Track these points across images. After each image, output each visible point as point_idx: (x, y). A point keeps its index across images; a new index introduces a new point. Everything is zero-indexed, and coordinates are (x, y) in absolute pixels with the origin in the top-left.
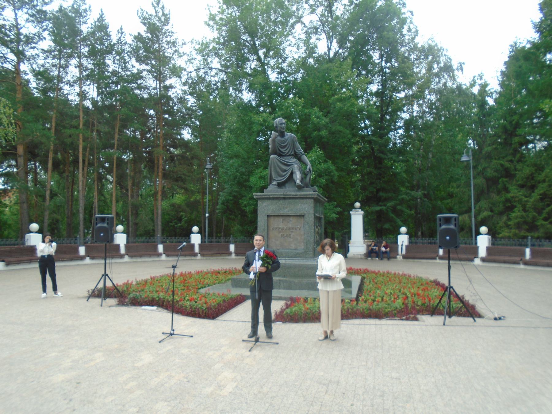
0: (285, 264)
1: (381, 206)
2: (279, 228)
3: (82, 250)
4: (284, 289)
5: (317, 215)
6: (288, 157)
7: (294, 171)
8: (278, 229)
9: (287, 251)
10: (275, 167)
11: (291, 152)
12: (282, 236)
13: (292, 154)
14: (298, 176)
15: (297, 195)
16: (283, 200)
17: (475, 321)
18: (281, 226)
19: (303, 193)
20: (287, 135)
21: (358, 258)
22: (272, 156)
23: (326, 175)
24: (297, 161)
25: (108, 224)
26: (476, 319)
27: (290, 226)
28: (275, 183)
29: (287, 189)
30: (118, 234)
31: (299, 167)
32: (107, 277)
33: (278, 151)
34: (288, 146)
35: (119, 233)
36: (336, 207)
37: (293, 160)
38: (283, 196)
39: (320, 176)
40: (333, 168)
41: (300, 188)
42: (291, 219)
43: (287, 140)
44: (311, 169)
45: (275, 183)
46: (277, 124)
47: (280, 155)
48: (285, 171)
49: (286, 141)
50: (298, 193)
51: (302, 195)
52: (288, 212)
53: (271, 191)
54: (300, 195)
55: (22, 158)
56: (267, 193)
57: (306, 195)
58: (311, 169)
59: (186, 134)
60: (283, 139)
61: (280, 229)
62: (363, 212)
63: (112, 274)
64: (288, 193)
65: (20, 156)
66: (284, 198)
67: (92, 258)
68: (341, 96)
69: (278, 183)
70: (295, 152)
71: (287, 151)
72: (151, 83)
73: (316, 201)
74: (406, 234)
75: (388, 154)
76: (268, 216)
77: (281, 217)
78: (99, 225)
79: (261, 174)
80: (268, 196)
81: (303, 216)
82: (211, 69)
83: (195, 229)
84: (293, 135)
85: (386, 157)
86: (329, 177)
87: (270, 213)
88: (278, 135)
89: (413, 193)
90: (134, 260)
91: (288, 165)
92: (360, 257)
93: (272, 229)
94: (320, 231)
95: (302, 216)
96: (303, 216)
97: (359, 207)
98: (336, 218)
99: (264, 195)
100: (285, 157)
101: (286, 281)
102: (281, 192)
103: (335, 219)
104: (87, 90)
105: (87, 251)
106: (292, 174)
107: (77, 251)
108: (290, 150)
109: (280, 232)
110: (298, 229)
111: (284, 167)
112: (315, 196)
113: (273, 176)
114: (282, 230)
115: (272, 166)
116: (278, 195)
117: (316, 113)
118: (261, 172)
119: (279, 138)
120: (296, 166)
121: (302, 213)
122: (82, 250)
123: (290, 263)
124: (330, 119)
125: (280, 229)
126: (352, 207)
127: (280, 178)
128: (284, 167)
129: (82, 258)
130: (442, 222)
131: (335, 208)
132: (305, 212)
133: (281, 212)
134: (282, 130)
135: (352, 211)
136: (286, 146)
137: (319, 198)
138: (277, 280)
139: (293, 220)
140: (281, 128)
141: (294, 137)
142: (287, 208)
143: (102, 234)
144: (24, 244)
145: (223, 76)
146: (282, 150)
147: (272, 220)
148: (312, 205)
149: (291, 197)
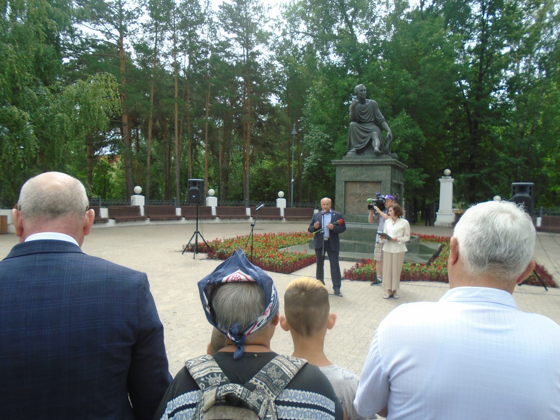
0: (361, 228)
1: (475, 173)
2: (357, 194)
3: (178, 212)
4: (358, 252)
5: (394, 181)
6: (368, 124)
7: (373, 138)
9: (364, 216)
10: (354, 134)
12: (359, 202)
13: (372, 120)
14: (377, 143)
16: (361, 167)
17: (547, 290)
18: (358, 192)
20: (368, 101)
21: (446, 227)
22: (351, 123)
23: (414, 140)
26: (548, 288)
27: (367, 192)
28: (353, 150)
29: (366, 156)
30: (210, 197)
31: (378, 133)
32: (198, 235)
33: (358, 118)
36: (422, 173)
37: (372, 127)
38: (360, 163)
39: (407, 141)
40: (421, 133)
41: (378, 155)
43: (368, 106)
44: (391, 135)
45: (353, 150)
46: (357, 91)
47: (360, 121)
48: (364, 138)
50: (376, 160)
51: (380, 162)
52: (365, 179)
53: (349, 158)
54: (377, 162)
55: (127, 126)
56: (345, 160)
57: (384, 162)
58: (391, 135)
59: (274, 100)
60: (364, 106)
62: (453, 179)
63: (202, 232)
64: (366, 160)
65: (125, 125)
66: (362, 165)
67: (187, 219)
68: (431, 56)
69: (357, 150)
70: (376, 119)
71: (367, 118)
73: (394, 167)
75: (485, 117)
76: (346, 182)
83: (281, 193)
84: (374, 101)
85: (482, 120)
86: (417, 143)
87: (347, 179)
88: (358, 102)
89: (512, 160)
90: (225, 221)
92: (448, 226)
94: (399, 198)
95: (379, 182)
97: (449, 174)
98: (423, 184)
99: (342, 162)
100: (365, 124)
101: (361, 244)
102: (359, 159)
103: (422, 186)
105: (183, 212)
106: (371, 140)
107: (174, 212)
109: (357, 198)
111: (363, 134)
112: (393, 163)
113: (352, 144)
115: (351, 133)
116: (357, 162)
117: (404, 75)
118: (345, 138)
119: (359, 105)
120: (375, 133)
121: (379, 179)
122: (178, 212)
123: (366, 227)
124: (420, 81)
126: (442, 174)
127: (359, 145)
128: (363, 134)
129: (179, 218)
130: (516, 191)
131: (421, 175)
132: (383, 179)
133: (358, 179)
135: (441, 178)
137: (398, 165)
138: (352, 243)
139: (370, 186)
140: (361, 94)
141: (375, 103)
142: (364, 175)
143: (194, 196)
144: (130, 204)
145: (310, 40)
146: (363, 117)
147: (349, 185)
148: (389, 172)
149: (368, 163)
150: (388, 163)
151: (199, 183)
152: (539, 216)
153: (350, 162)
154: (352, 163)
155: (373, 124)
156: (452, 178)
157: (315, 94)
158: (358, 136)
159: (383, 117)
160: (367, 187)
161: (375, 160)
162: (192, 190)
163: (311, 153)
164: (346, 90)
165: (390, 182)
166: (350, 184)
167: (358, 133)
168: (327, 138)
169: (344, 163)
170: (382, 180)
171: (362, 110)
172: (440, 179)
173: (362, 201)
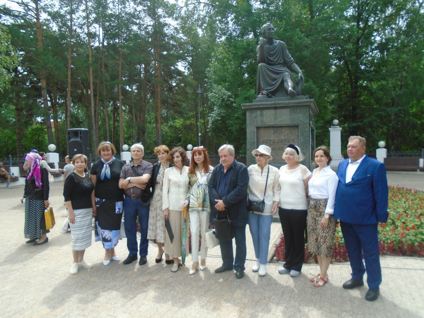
1: (357, 122)
6: (277, 66)
7: (285, 79)
8: (268, 142)
11: (280, 61)
13: (281, 62)
14: (290, 85)
15: (290, 103)
18: (272, 138)
19: (297, 101)
20: (276, 42)
22: (260, 64)
24: (288, 70)
25: (81, 139)
27: (283, 138)
30: (124, 152)
34: (277, 54)
35: (125, 151)
38: (274, 106)
41: (292, 95)
43: (276, 47)
47: (270, 63)
48: (275, 79)
49: (275, 48)
52: (279, 123)
53: (260, 101)
54: (293, 103)
55: (45, 90)
56: (255, 103)
57: (301, 103)
59: (181, 66)
60: (271, 47)
61: (272, 142)
62: (341, 128)
65: (43, 89)
68: (323, 16)
70: (284, 59)
71: (276, 59)
72: (148, 21)
74: (385, 147)
75: (365, 73)
76: (257, 128)
77: (272, 128)
78: (72, 140)
79: (246, 95)
81: (297, 126)
84: (282, 42)
85: (363, 76)
87: (259, 124)
88: (266, 41)
89: (389, 109)
93: (262, 141)
96: (297, 126)
102: (271, 102)
106: (283, 82)
108: (279, 57)
111: (274, 76)
114: (274, 142)
116: (268, 104)
119: (267, 46)
120: (287, 73)
121: (296, 123)
125: (272, 142)
126: (330, 123)
128: (274, 76)
132: (300, 122)
134: (270, 36)
135: (330, 127)
136: (275, 53)
139: (286, 131)
140: (269, 33)
141: (283, 44)
146: (271, 58)
147: (262, 131)
149: (283, 105)
150: (306, 104)
151: (81, 132)
152: (421, 158)
153: (261, 105)
154: (264, 106)
155: (283, 66)
156: (340, 127)
157: (217, 60)
158: (267, 77)
159: (292, 59)
160: (282, 132)
161: (291, 101)
162: (73, 141)
163: (215, 109)
164: (245, 49)
166: (262, 130)
168: (228, 95)
169: (255, 107)
170: (299, 124)
171: (270, 51)
172: (330, 129)
173: (277, 148)
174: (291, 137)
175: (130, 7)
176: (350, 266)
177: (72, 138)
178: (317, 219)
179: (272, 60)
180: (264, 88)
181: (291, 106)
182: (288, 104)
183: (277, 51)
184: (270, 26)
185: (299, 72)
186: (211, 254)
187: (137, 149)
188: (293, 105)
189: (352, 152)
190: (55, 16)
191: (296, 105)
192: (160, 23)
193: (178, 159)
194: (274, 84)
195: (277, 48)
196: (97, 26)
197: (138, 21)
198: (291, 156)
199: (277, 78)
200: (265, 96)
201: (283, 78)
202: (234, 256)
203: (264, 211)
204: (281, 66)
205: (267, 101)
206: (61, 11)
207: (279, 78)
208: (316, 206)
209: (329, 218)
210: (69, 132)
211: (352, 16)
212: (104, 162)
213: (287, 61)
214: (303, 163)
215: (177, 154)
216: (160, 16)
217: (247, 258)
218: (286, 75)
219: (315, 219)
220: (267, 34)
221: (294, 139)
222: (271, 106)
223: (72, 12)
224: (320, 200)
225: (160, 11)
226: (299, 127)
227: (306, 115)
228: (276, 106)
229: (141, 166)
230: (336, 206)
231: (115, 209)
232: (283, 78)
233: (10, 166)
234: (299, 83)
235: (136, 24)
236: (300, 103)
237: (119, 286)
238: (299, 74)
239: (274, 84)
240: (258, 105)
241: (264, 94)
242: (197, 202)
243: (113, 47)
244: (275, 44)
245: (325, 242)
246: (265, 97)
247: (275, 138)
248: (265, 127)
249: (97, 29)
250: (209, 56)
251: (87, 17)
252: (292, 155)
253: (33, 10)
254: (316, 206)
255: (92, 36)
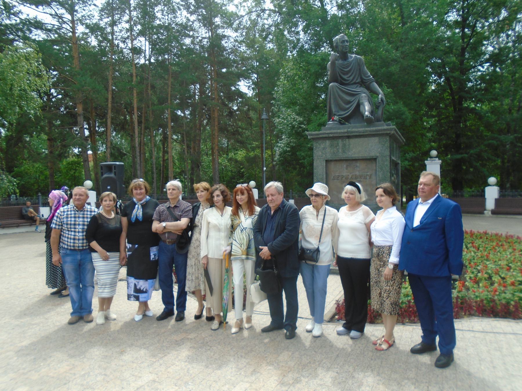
1: (462, 154)
2: (343, 177)
5: (393, 158)
7: (361, 101)
8: (340, 178)
11: (357, 80)
13: (357, 81)
14: (367, 109)
15: (366, 131)
18: (344, 174)
19: (374, 129)
20: (352, 57)
22: (331, 84)
23: (397, 118)
24: (366, 91)
25: (115, 174)
27: (357, 173)
31: (368, 96)
33: (339, 78)
34: (352, 71)
38: (346, 135)
41: (369, 122)
42: (358, 165)
43: (351, 63)
45: (336, 118)
48: (349, 102)
49: (351, 64)
51: (373, 131)
52: (353, 156)
53: (330, 129)
54: (370, 131)
55: (82, 117)
56: (324, 131)
57: (379, 130)
60: (346, 63)
62: (441, 161)
64: (354, 130)
65: (79, 115)
70: (361, 78)
71: (351, 78)
72: (203, 33)
73: (392, 137)
75: (472, 92)
76: (327, 161)
77: (344, 162)
78: (105, 176)
79: (321, 121)
80: (326, 135)
82: (263, 11)
86: (400, 121)
87: (329, 157)
88: (338, 56)
89: (502, 137)
91: (353, 95)
95: (373, 160)
97: (435, 156)
99: (321, 134)
102: (343, 130)
104: (139, 45)
106: (359, 105)
110: (368, 177)
111: (348, 98)
112: (392, 132)
113: (334, 110)
116: (340, 133)
117: (384, 46)
118: (320, 119)
119: (340, 62)
120: (364, 95)
124: (402, 53)
125: (344, 178)
126: (427, 155)
128: (348, 98)
134: (344, 50)
135: (427, 160)
137: (397, 135)
139: (361, 165)
140: (343, 46)
145: (277, 18)
146: (345, 77)
147: (332, 166)
148: (388, 144)
149: (357, 134)
150: (386, 132)
151: (115, 167)
154: (335, 135)
155: (359, 86)
156: (439, 159)
157: (287, 77)
158: (340, 100)
159: (372, 77)
160: (357, 166)
161: (367, 129)
162: (106, 178)
163: (283, 137)
164: (319, 65)
165: (388, 159)
166: (333, 163)
167: (339, 96)
168: (299, 121)
169: (324, 136)
170: (377, 157)
171: (344, 68)
172: (426, 162)
174: (367, 172)
175: (183, 16)
176: (420, 328)
177: (105, 173)
178: (380, 269)
179: (347, 79)
180: (335, 113)
181: (368, 135)
182: (363, 132)
183: (352, 67)
184: (344, 38)
185: (379, 93)
186: (261, 311)
187: (172, 187)
188: (370, 133)
189: (425, 190)
190: (94, 29)
191: (373, 133)
192: (218, 35)
193: (218, 198)
194: (348, 108)
195: (352, 65)
196: (142, 39)
197: (191, 33)
198: (351, 196)
199: (351, 100)
200: (336, 122)
201: (359, 101)
202: (285, 313)
203: (320, 260)
204: (357, 86)
205: (339, 129)
206: (101, 22)
207: (354, 100)
208: (378, 254)
209: (394, 268)
210: (102, 167)
211: (456, 22)
212: (136, 202)
213: (366, 80)
214: (365, 203)
215: (217, 192)
216: (218, 27)
217: (299, 315)
218: (362, 97)
219: (378, 270)
220: (340, 48)
221: (371, 175)
222: (343, 135)
223: (113, 24)
224: (383, 247)
225: (218, 20)
226: (377, 160)
227: (386, 145)
228: (349, 134)
229: (178, 207)
230: (402, 253)
231: (150, 256)
232: (359, 101)
233: (39, 207)
234: (379, 106)
235: (189, 36)
236: (378, 131)
237: (148, 344)
238: (380, 96)
239: (348, 108)
240: (327, 134)
241: (336, 121)
242: (240, 249)
243: (161, 64)
244: (350, 60)
245: (389, 296)
246: (336, 124)
247: (349, 174)
248: (336, 161)
249: (142, 43)
250: (277, 74)
251: (131, 30)
252: (352, 194)
253: (69, 23)
254: (378, 254)
255: (136, 51)
